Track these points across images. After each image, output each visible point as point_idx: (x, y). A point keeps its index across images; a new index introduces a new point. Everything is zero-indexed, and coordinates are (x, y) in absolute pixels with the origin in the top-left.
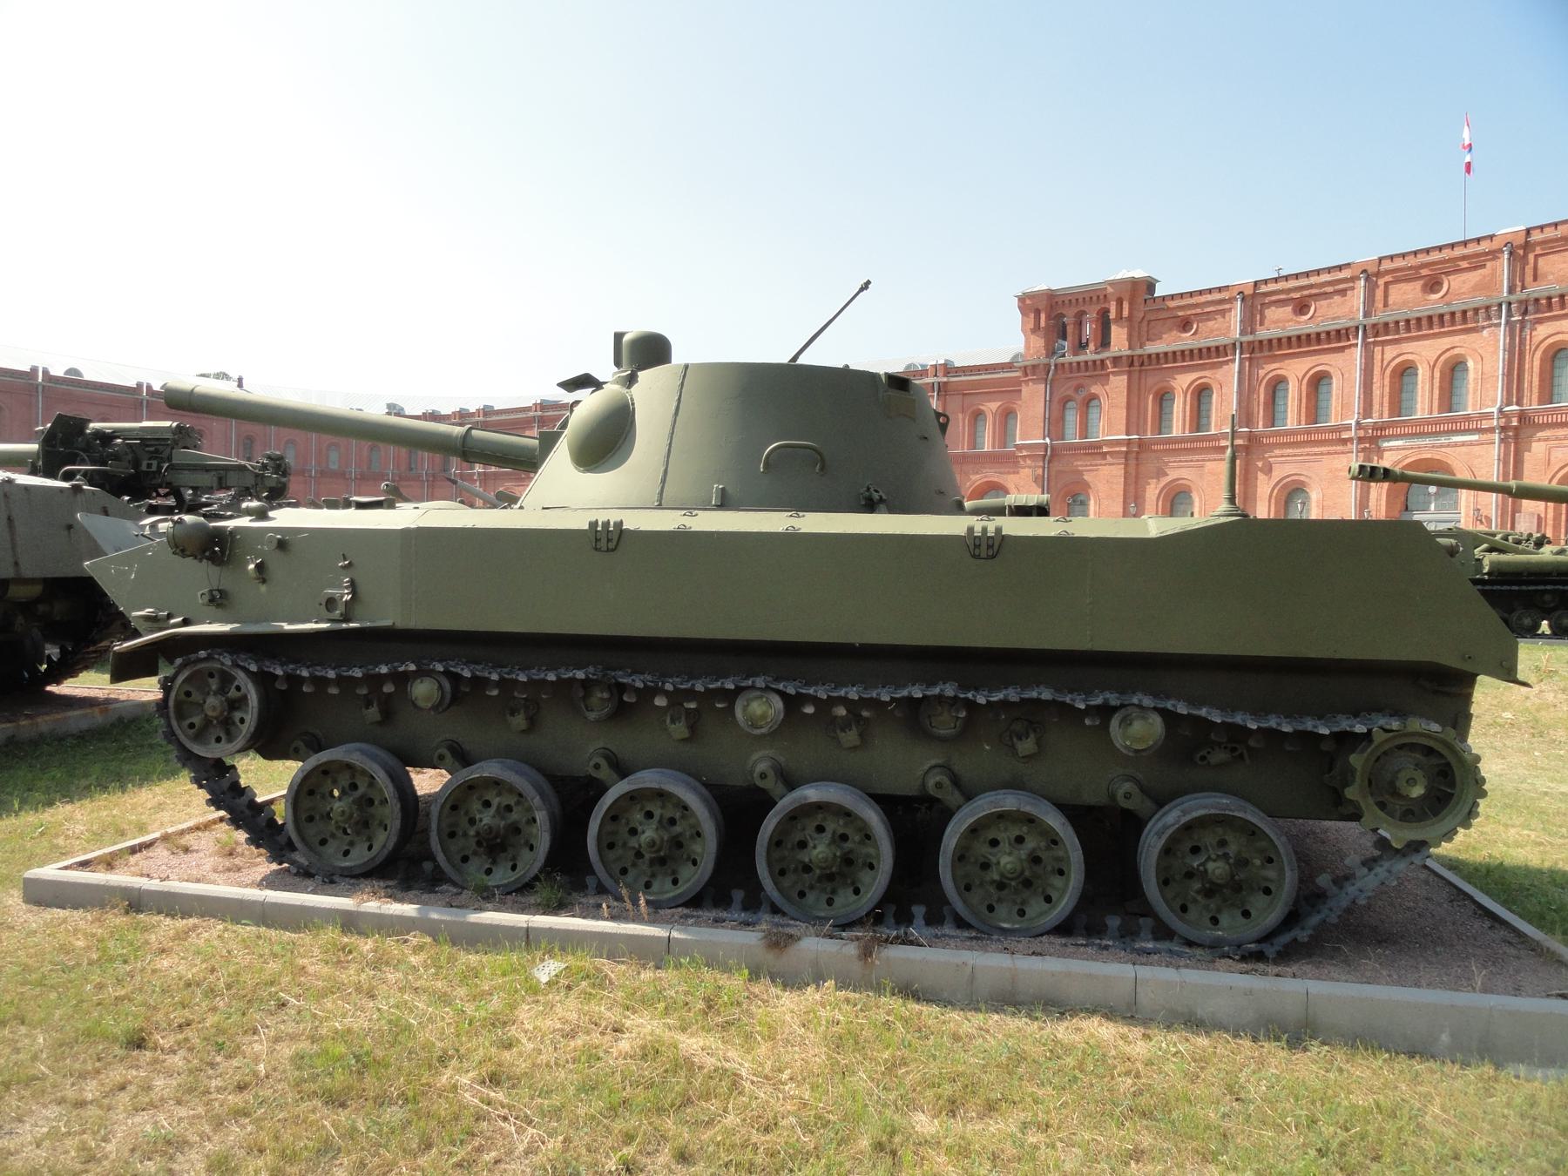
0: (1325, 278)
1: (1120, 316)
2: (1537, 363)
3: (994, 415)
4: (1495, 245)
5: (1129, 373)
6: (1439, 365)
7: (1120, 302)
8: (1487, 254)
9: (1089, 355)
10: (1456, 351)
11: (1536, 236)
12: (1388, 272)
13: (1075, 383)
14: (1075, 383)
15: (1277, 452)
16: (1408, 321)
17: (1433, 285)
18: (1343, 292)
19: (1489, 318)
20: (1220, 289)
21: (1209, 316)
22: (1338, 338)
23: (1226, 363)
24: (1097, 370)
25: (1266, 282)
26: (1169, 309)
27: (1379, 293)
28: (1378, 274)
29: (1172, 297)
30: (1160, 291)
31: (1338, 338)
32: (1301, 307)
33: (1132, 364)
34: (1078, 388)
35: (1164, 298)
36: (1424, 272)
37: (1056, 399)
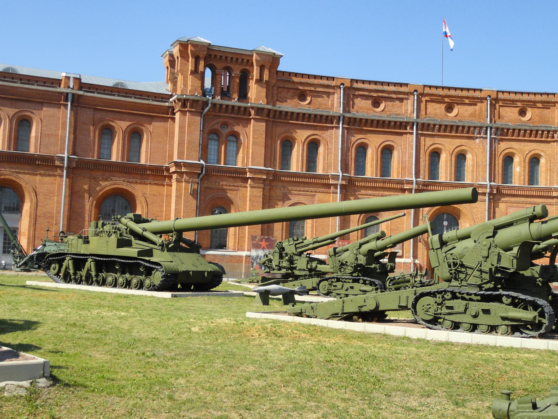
0: (392, 88)
2: (501, 161)
3: (124, 133)
6: (454, 154)
7: (262, 68)
8: (478, 98)
9: (234, 101)
10: (463, 148)
11: (501, 96)
12: (428, 95)
14: (221, 120)
15: (363, 192)
17: (449, 109)
18: (401, 100)
19: (480, 133)
20: (328, 78)
21: (318, 94)
22: (399, 127)
23: (332, 128)
24: (242, 115)
25: (357, 81)
26: (293, 82)
27: (423, 105)
28: (423, 95)
29: (296, 75)
31: (399, 127)
32: (376, 103)
33: (268, 115)
34: (225, 125)
36: (447, 100)
37: (206, 131)
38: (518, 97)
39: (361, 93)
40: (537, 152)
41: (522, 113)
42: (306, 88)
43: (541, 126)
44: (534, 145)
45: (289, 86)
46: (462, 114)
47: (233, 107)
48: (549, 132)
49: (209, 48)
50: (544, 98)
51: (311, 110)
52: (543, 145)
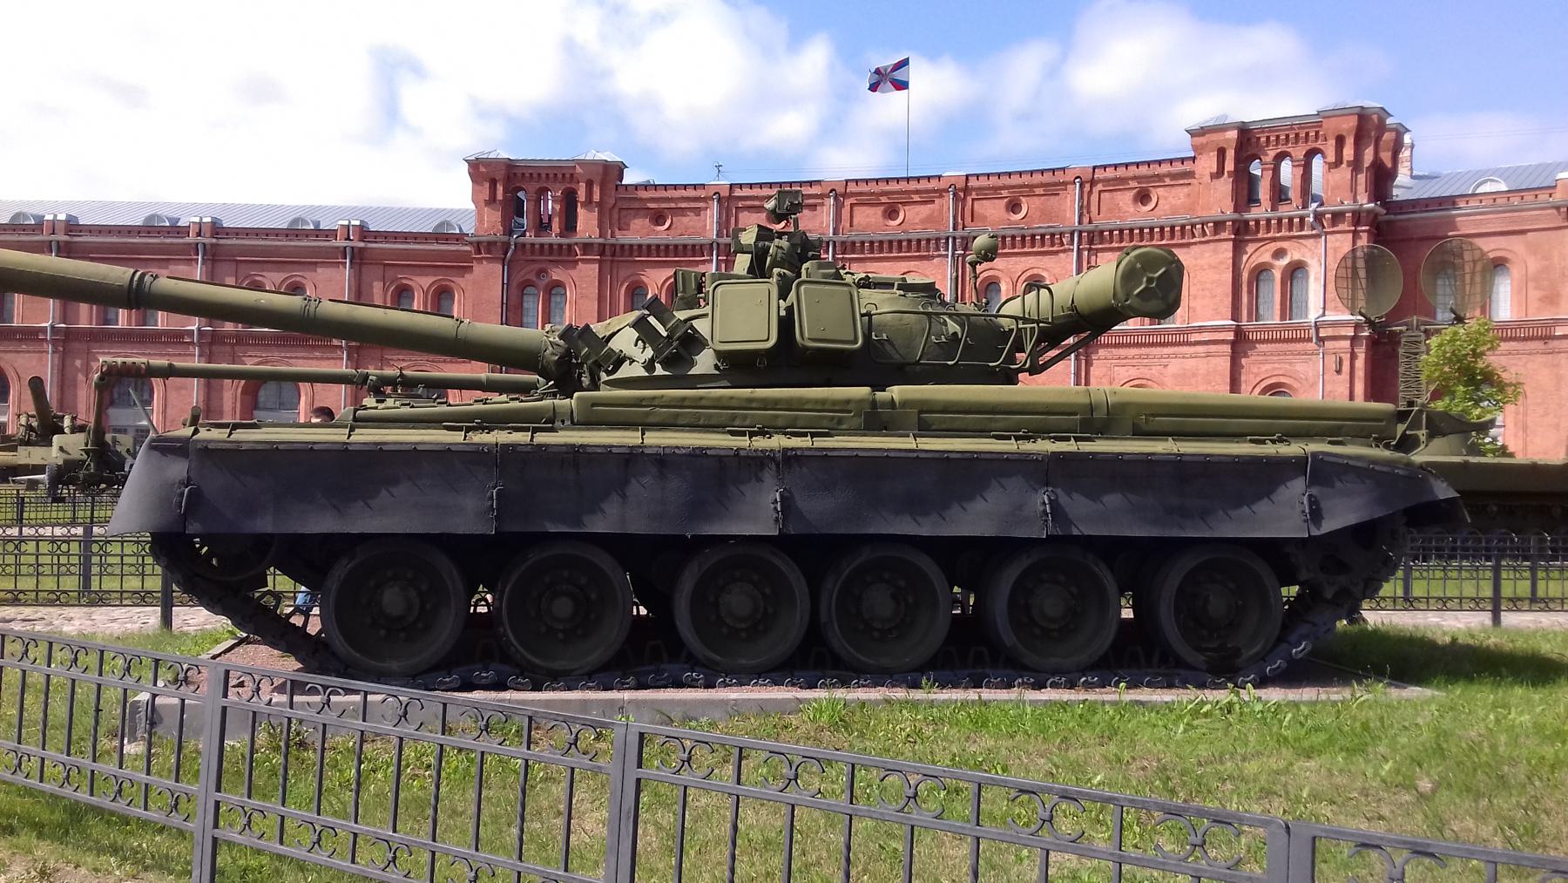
1: (589, 202)
3: (426, 294)
4: (943, 185)
5: (600, 262)
7: (590, 184)
8: (934, 191)
9: (553, 238)
12: (853, 194)
13: (537, 266)
14: (537, 266)
16: (872, 243)
17: (891, 213)
20: (695, 187)
21: (682, 212)
24: (565, 255)
25: (741, 186)
27: (846, 212)
28: (845, 195)
30: (629, 178)
35: (636, 187)
36: (884, 199)
37: (514, 284)
38: (1005, 181)
39: (749, 203)
40: (1035, 271)
41: (1014, 207)
42: (664, 205)
43: (1040, 226)
44: (1031, 260)
45: (636, 205)
46: (913, 218)
47: (551, 245)
48: (1053, 235)
49: (510, 165)
50: (1047, 178)
51: (672, 239)
52: (1046, 258)
